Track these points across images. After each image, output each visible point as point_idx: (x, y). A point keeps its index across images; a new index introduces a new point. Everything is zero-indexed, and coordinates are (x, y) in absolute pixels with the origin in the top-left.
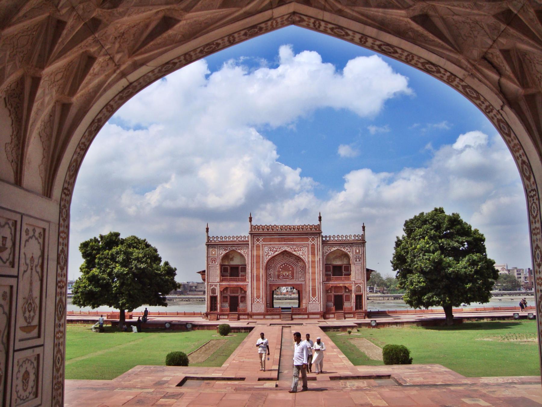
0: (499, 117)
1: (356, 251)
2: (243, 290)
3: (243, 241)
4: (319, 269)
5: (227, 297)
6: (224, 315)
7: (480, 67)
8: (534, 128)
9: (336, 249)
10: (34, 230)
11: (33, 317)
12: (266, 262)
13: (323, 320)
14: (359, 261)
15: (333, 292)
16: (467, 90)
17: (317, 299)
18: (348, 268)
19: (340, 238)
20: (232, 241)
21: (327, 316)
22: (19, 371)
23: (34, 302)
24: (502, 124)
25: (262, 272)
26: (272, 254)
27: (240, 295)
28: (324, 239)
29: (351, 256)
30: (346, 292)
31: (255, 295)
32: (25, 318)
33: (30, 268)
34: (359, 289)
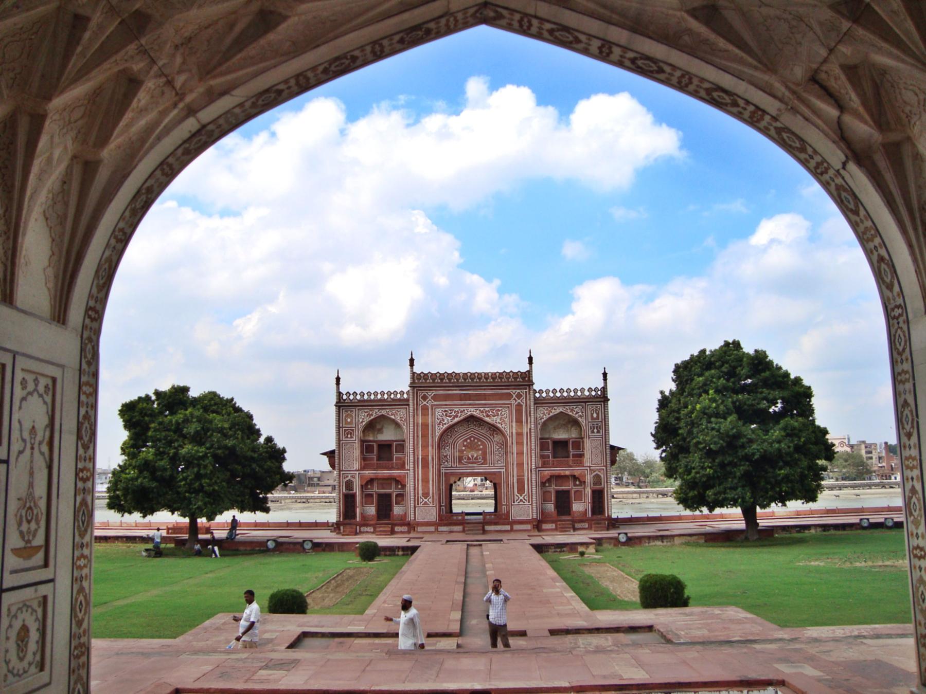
0: (839, 181)
1: (592, 415)
2: (399, 482)
3: (399, 400)
5: (372, 495)
6: (367, 525)
7: (805, 95)
8: (899, 201)
9: (558, 411)
10: (36, 381)
11: (36, 530)
12: (438, 434)
13: (537, 533)
14: (598, 432)
15: (553, 486)
16: (785, 135)
17: (526, 498)
18: (578, 444)
19: (565, 394)
20: (380, 400)
21: (545, 526)
22: (10, 626)
23: (36, 505)
24: (843, 194)
25: (432, 452)
27: (393, 491)
28: (537, 395)
30: (575, 485)
31: (421, 492)
32: (21, 533)
33: (29, 446)
34: (597, 480)
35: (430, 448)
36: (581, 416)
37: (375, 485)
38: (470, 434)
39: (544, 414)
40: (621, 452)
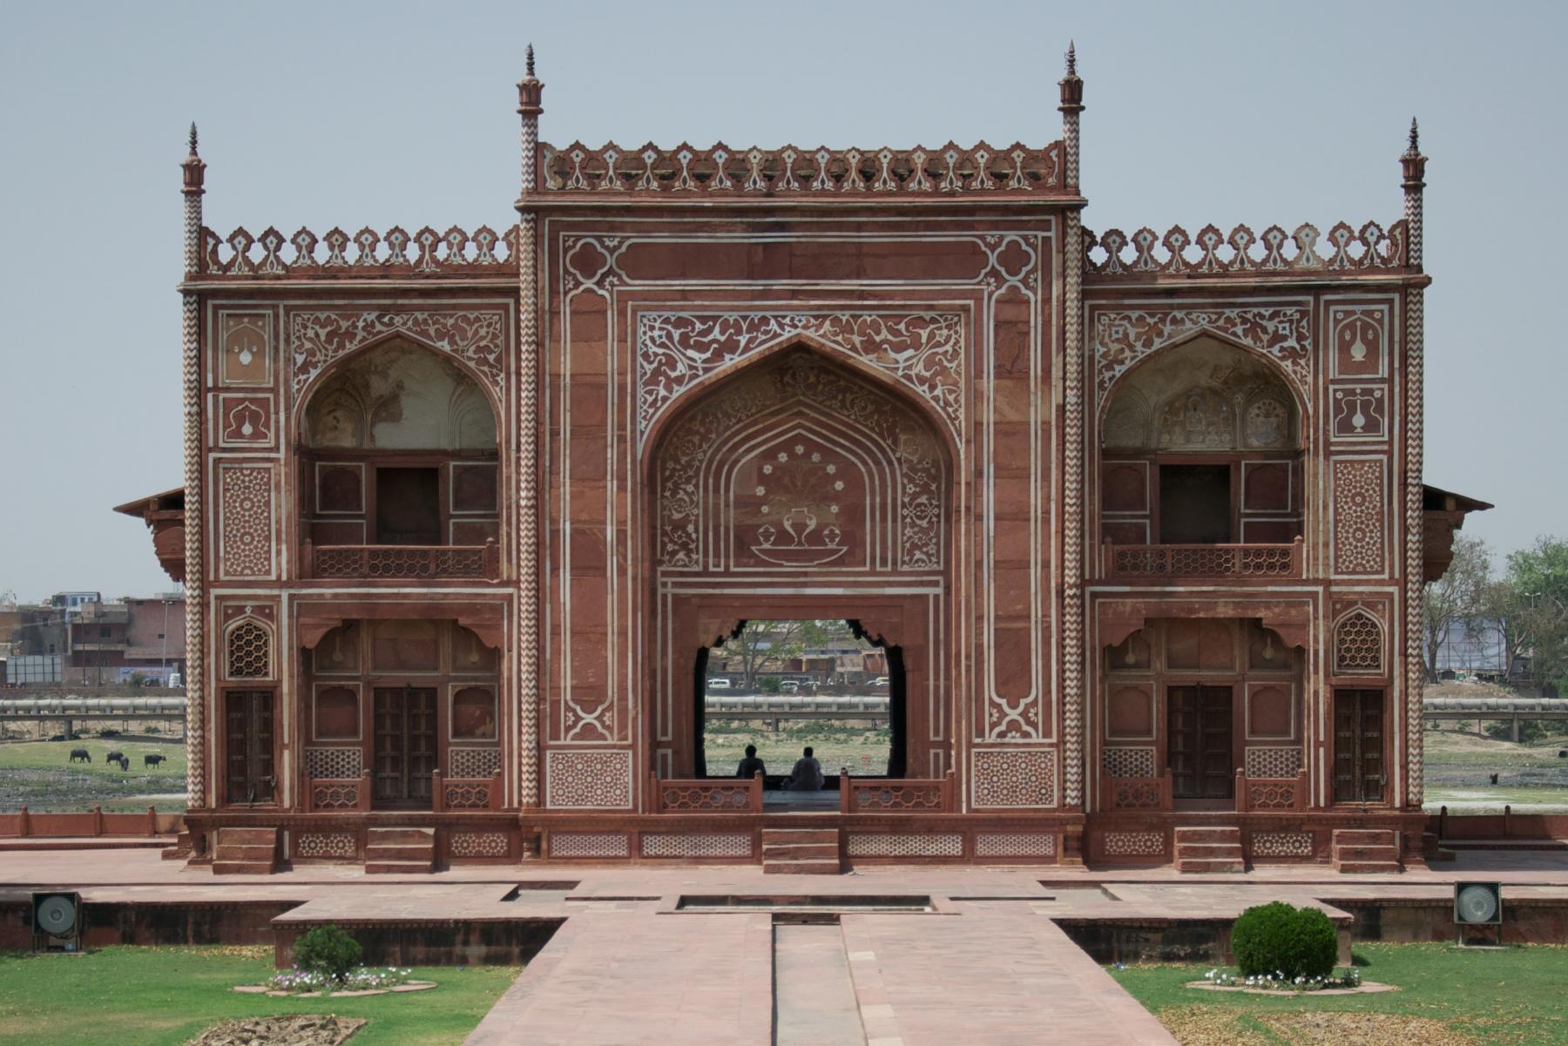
3: (474, 270)
4: (1057, 490)
6: (327, 828)
12: (647, 428)
14: (1372, 426)
15: (1159, 664)
17: (1037, 714)
19: (1225, 253)
20: (386, 270)
21: (1116, 842)
25: (618, 507)
26: (694, 368)
27: (447, 678)
28: (1098, 255)
29: (1306, 391)
31: (567, 682)
35: (612, 486)
36: (1292, 354)
37: (365, 644)
38: (787, 429)
39: (1126, 339)
40: (1471, 518)
